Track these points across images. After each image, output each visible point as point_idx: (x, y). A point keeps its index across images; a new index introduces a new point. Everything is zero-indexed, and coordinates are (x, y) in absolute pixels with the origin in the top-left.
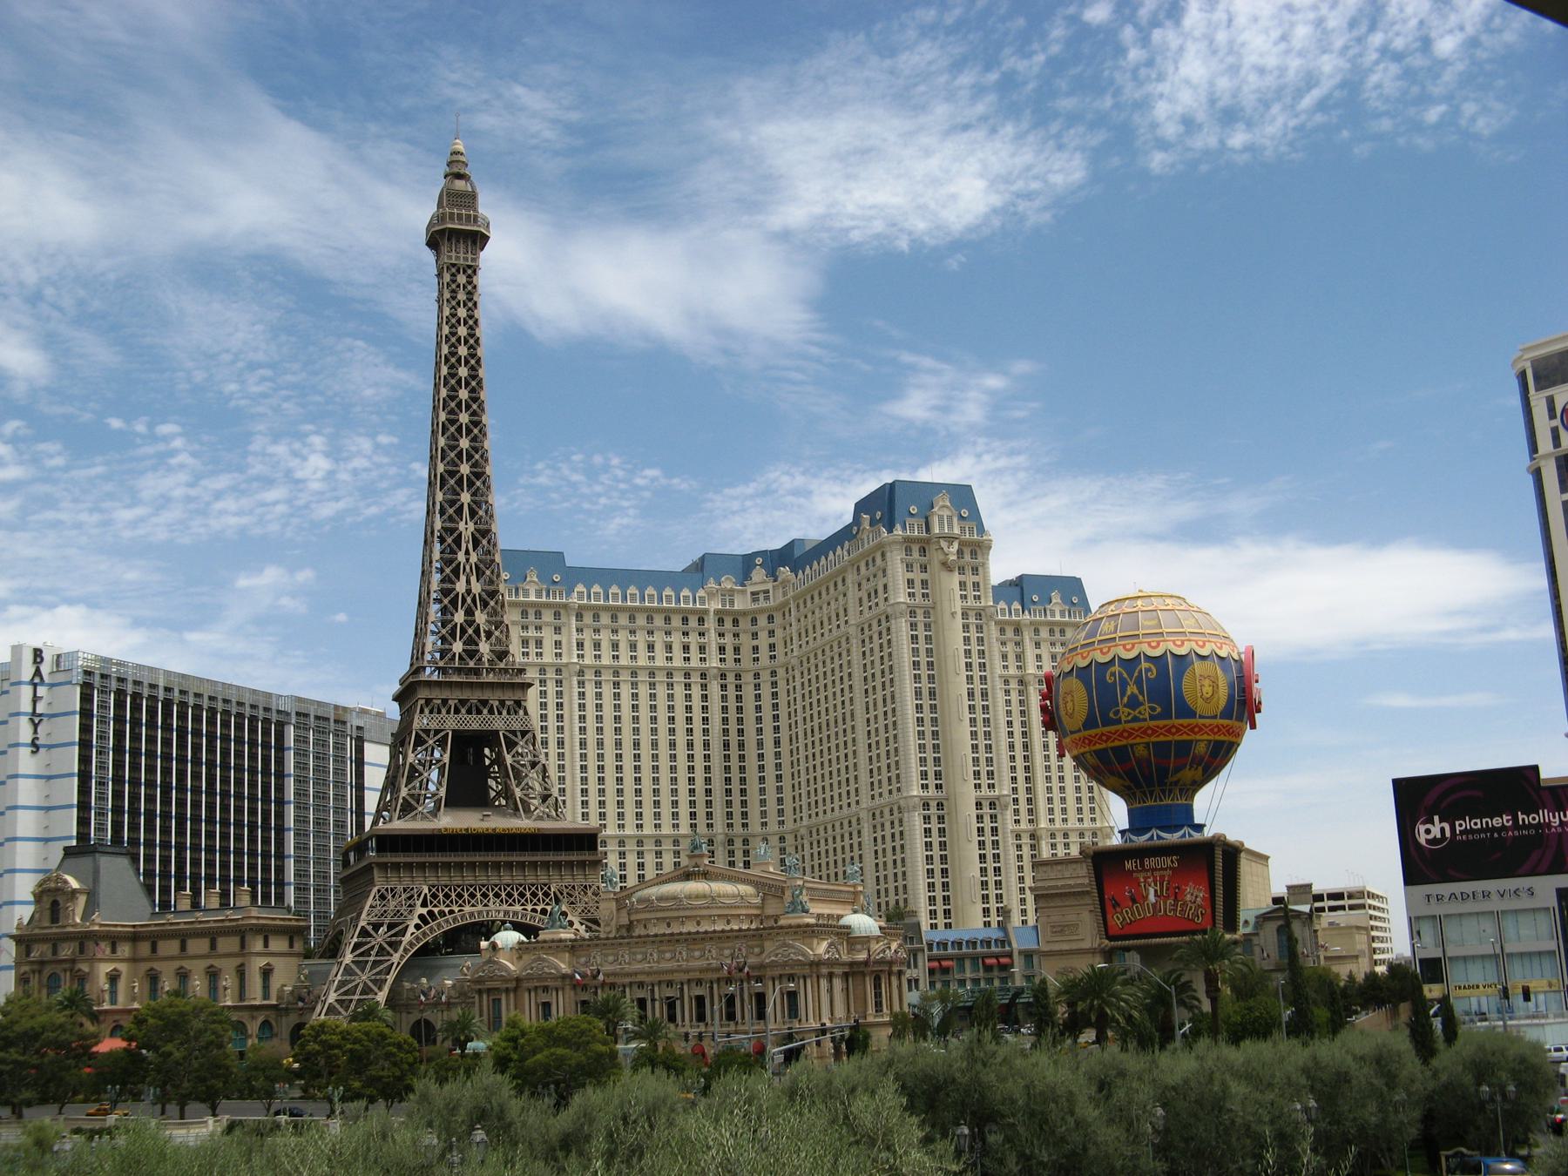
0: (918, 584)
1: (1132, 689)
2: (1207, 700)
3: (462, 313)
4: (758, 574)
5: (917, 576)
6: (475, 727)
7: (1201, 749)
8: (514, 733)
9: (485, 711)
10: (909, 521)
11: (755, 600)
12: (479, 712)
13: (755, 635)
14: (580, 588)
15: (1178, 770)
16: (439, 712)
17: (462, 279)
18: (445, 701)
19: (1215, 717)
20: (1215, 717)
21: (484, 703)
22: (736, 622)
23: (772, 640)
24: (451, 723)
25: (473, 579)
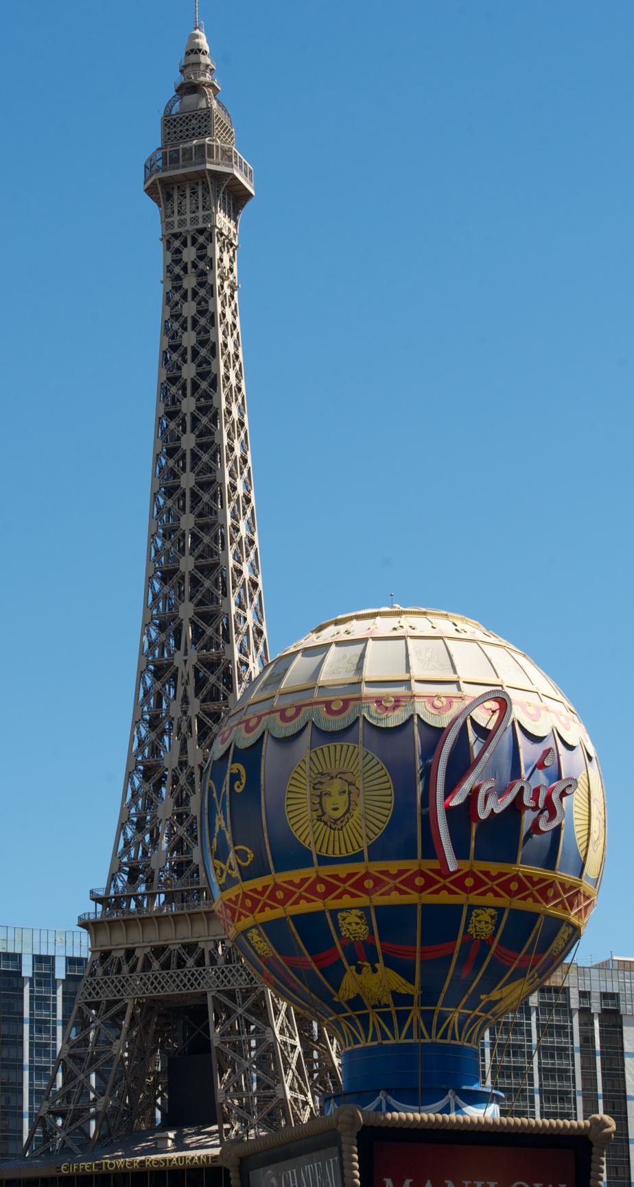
1: (220, 822)
2: (335, 824)
3: (189, 309)
6: (171, 990)
7: (353, 926)
8: (231, 995)
9: (190, 962)
12: (181, 964)
15: (335, 974)
16: (119, 971)
17: (189, 254)
18: (130, 953)
19: (358, 857)
20: (358, 857)
21: (190, 948)
24: (136, 989)
25: (192, 744)
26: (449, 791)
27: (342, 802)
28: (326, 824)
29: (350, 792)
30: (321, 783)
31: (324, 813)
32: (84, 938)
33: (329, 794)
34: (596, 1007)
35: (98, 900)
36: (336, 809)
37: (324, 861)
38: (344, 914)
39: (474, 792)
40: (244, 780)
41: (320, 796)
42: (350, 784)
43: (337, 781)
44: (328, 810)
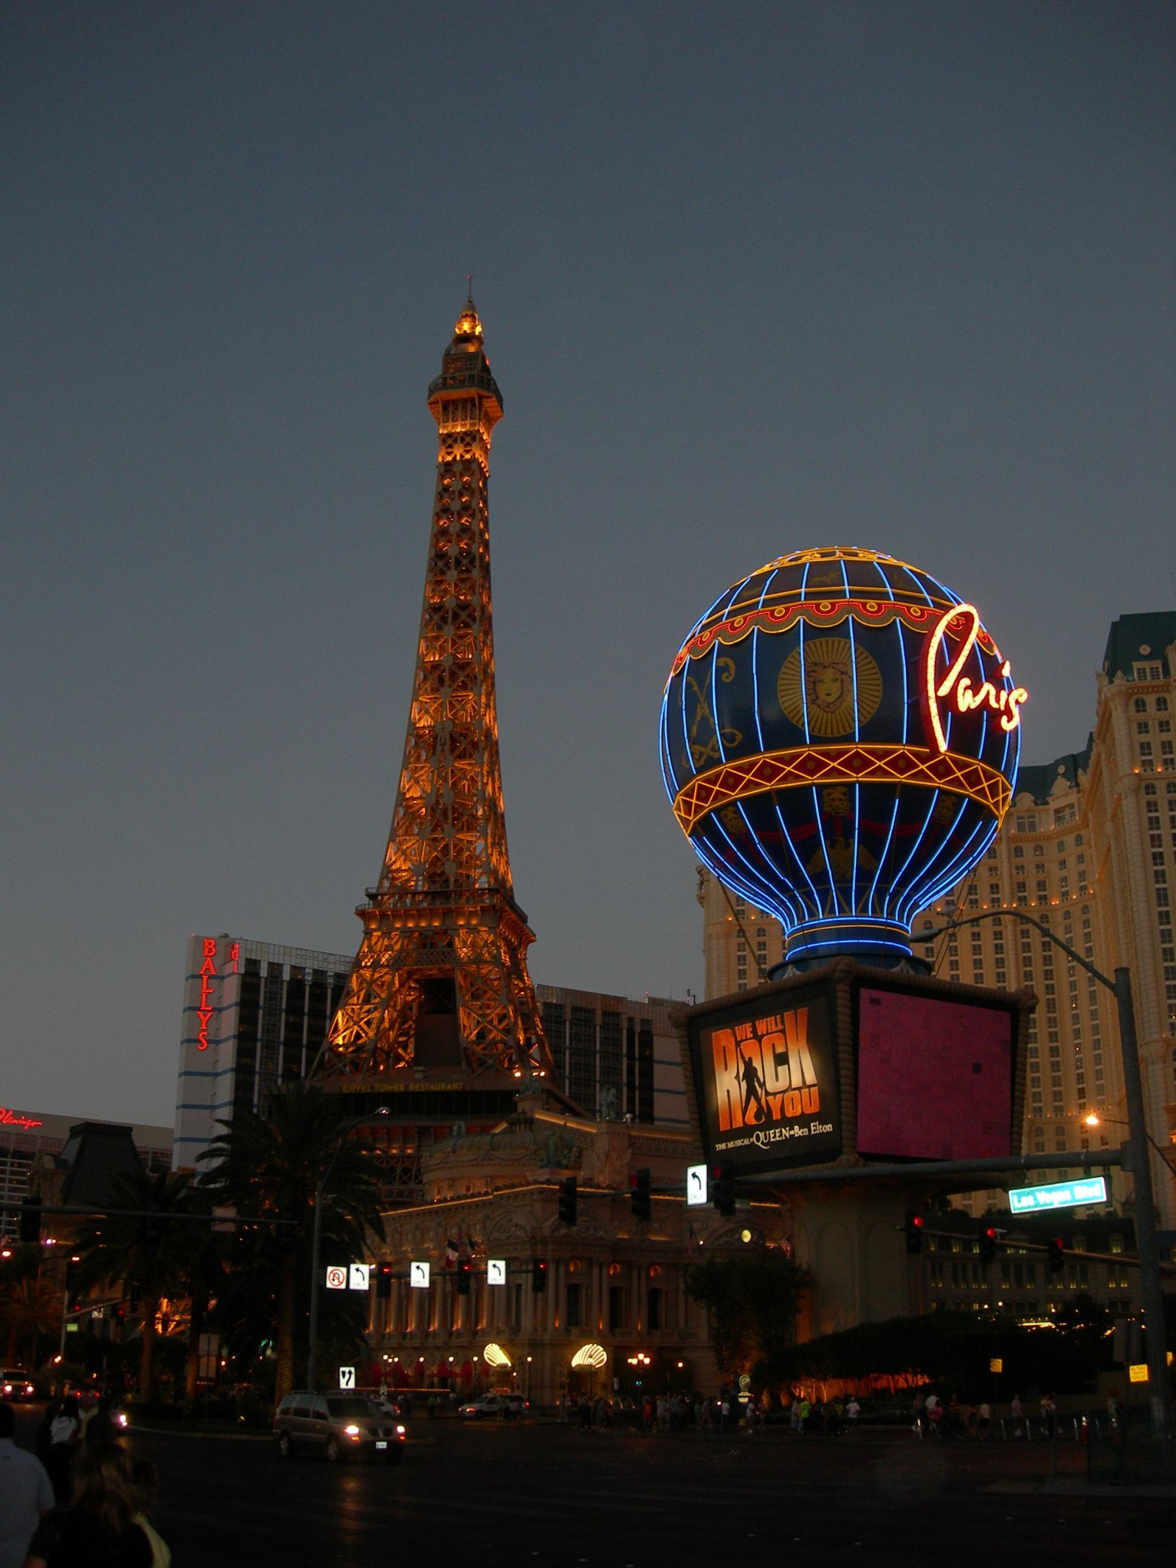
0: (1156, 748)
4: (1061, 785)
5: (1155, 737)
10: (1136, 665)
11: (1058, 819)
13: (1063, 864)
19: (849, 739)
22: (1039, 849)
23: (1081, 867)
26: (938, 686)
27: (835, 689)
29: (842, 681)
30: (814, 671)
31: (817, 698)
32: (360, 923)
33: (822, 681)
34: (638, 1029)
35: (372, 897)
37: (815, 740)
38: (829, 791)
39: (954, 689)
40: (733, 671)
41: (814, 683)
42: (842, 673)
43: (830, 671)
44: (822, 695)
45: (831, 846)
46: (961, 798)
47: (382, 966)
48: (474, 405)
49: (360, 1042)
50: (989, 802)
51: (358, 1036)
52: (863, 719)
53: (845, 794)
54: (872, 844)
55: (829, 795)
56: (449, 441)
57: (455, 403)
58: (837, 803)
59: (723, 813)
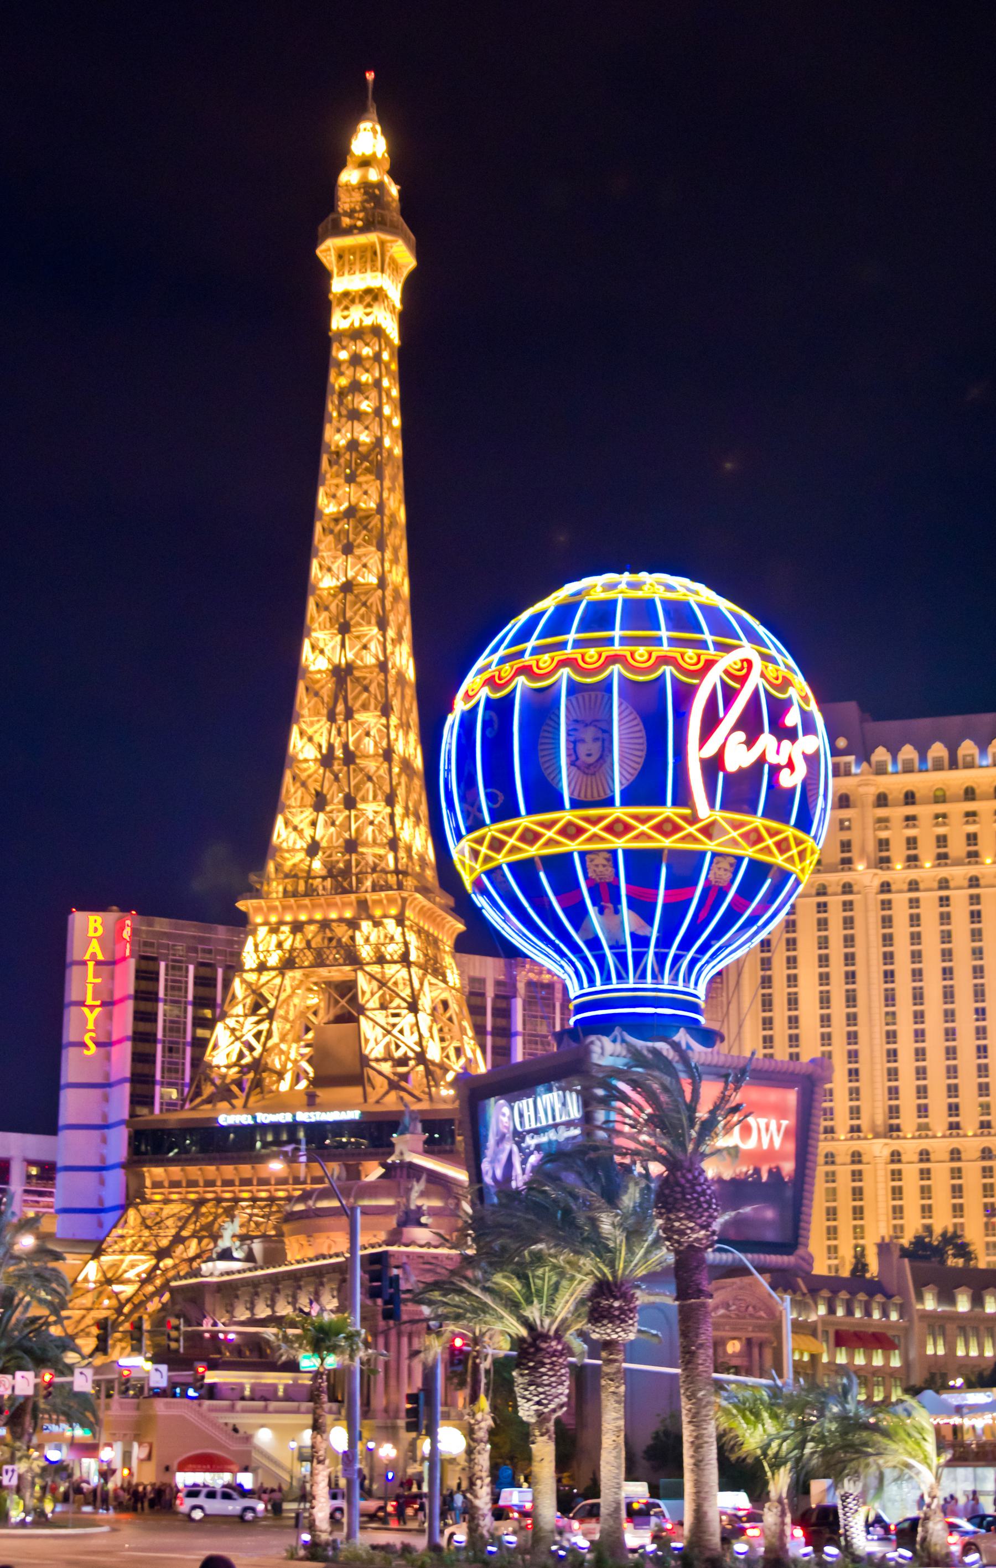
14: (881, 754)
19: (610, 802)
27: (595, 748)
28: (579, 768)
29: (603, 740)
31: (577, 759)
36: (589, 755)
37: (576, 804)
40: (496, 726)
44: (583, 757)
45: (601, 911)
46: (740, 859)
47: (273, 969)
48: (375, 253)
49: (244, 1062)
50: (779, 860)
51: (241, 1055)
52: (624, 781)
53: (608, 860)
54: (643, 909)
55: (592, 860)
56: (345, 303)
57: (352, 250)
58: (601, 868)
59: (493, 876)
